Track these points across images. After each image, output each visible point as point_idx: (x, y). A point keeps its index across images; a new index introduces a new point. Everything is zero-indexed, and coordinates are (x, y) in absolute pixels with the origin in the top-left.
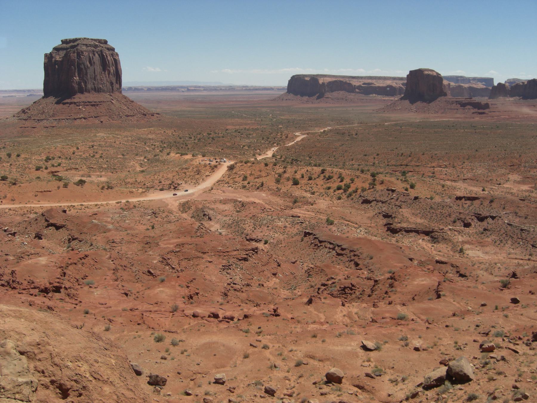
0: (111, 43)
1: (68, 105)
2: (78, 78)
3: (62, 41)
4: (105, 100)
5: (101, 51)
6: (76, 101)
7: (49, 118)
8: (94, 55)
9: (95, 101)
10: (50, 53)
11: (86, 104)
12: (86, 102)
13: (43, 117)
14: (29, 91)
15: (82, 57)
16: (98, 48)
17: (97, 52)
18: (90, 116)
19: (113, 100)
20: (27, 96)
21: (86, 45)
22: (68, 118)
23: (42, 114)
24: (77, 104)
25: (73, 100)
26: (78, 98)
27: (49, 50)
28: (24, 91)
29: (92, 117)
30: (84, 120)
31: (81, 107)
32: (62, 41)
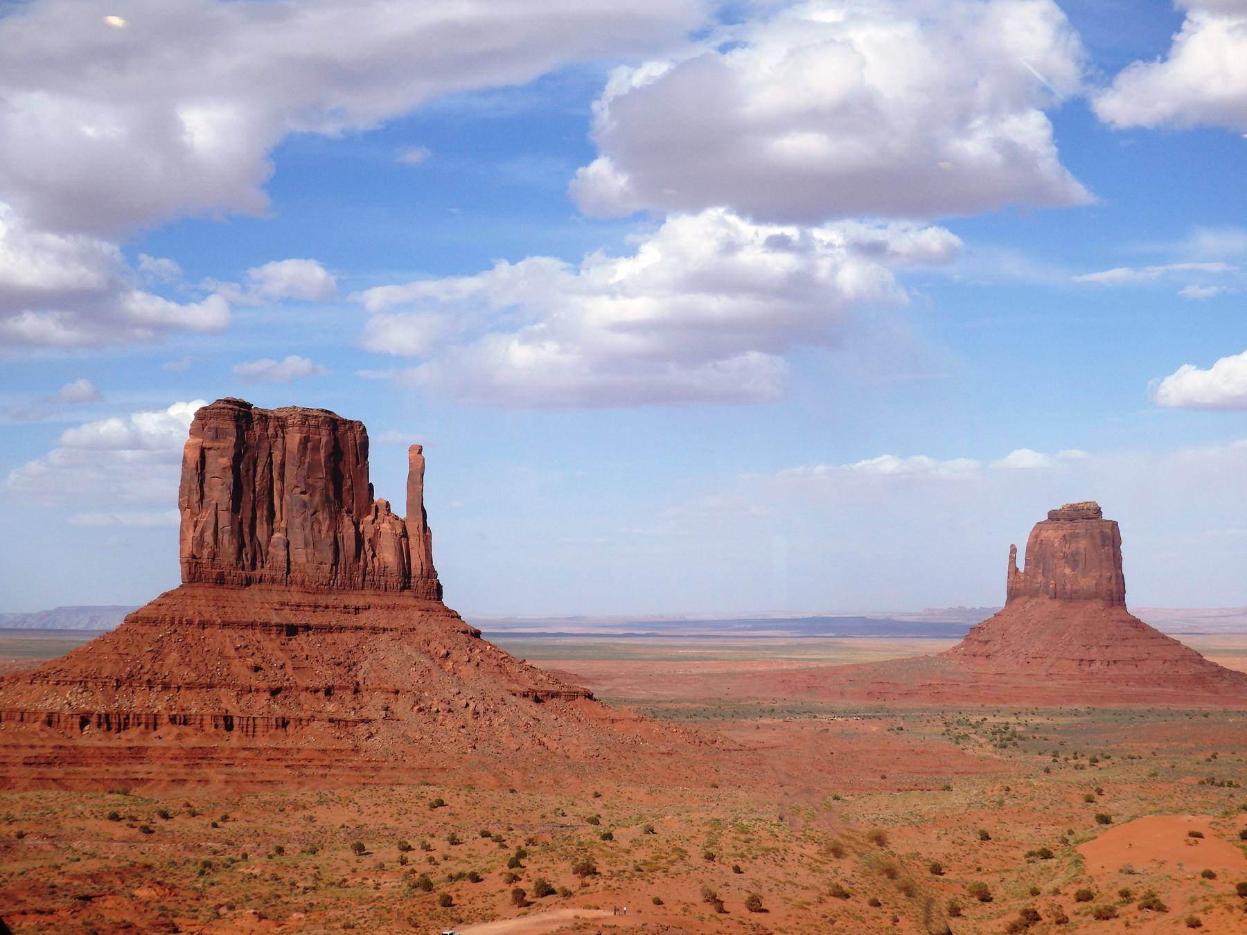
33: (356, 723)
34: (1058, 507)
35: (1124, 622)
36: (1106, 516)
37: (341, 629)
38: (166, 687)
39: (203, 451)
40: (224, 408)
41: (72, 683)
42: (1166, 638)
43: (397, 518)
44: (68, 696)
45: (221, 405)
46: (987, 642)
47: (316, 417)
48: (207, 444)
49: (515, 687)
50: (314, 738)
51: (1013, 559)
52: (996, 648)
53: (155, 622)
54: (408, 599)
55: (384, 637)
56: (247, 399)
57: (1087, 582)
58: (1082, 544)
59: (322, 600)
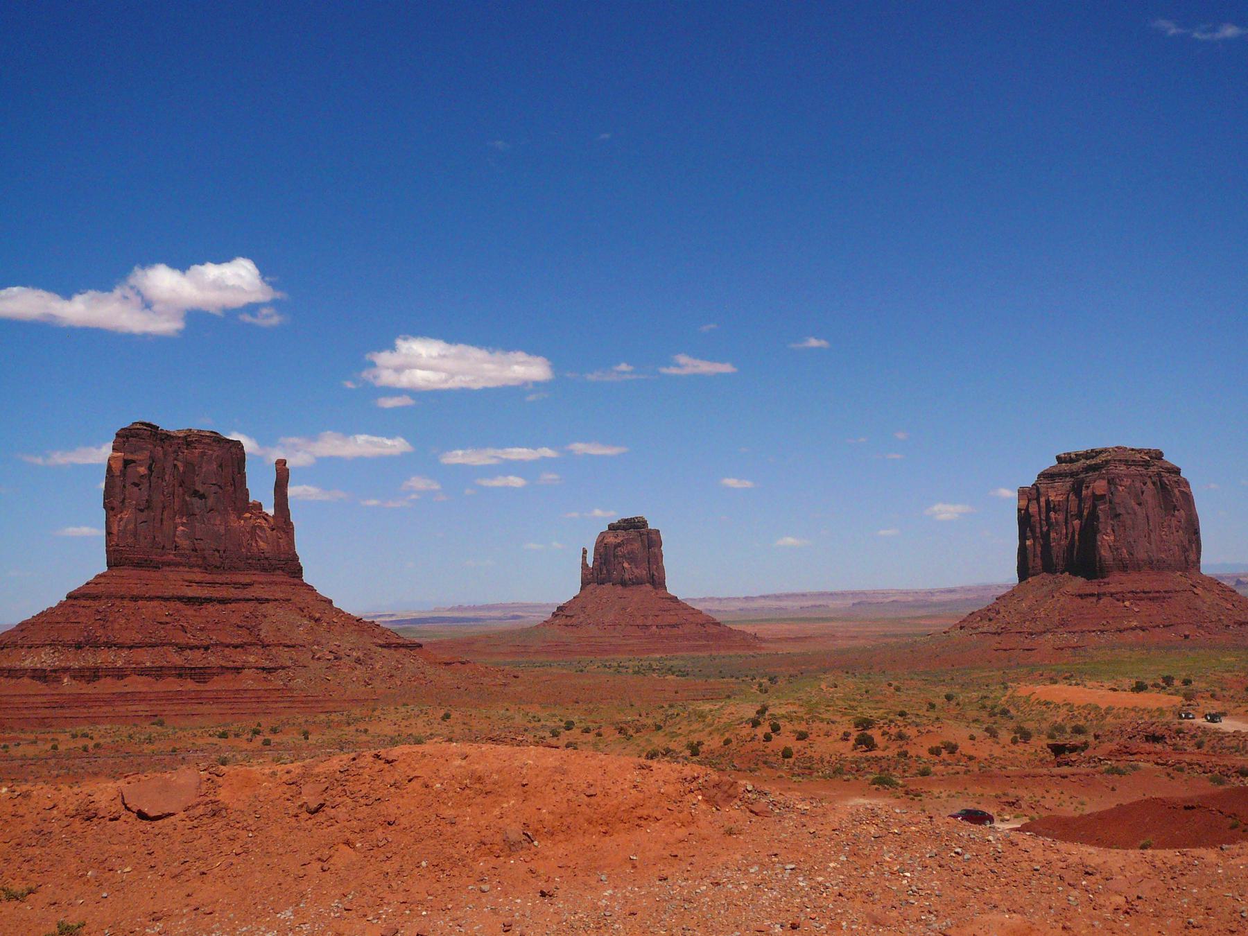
0: (1171, 458)
1: (1094, 599)
2: (1112, 538)
3: (1058, 458)
4: (1178, 589)
5: (1159, 474)
6: (1113, 591)
7: (1059, 630)
8: (1145, 484)
9: (1156, 589)
10: (1034, 485)
11: (1137, 596)
12: (1136, 593)
13: (1040, 626)
14: (854, 594)
15: (1120, 488)
16: (1152, 469)
17: (1150, 477)
18: (1154, 624)
19: (1195, 587)
20: (854, 604)
21: (1126, 462)
22: (1102, 627)
23: (1034, 620)
24: (1117, 596)
25: (1104, 589)
26: (1117, 582)
27: (1030, 481)
28: (843, 595)
29: (1158, 626)
30: (1141, 633)
31: (1127, 603)
32: (1058, 458)
33: (275, 669)
34: (615, 521)
35: (668, 598)
36: (650, 527)
37: (237, 600)
38: (121, 646)
39: (127, 463)
40: (138, 429)
41: (44, 645)
42: (694, 609)
43: (267, 515)
44: (43, 656)
45: (138, 426)
46: (572, 616)
47: (208, 436)
48: (130, 457)
49: (375, 640)
50: (249, 681)
51: (584, 558)
52: (580, 620)
53: (96, 597)
54: (280, 577)
55: (269, 606)
56: (154, 423)
57: (641, 572)
58: (637, 546)
59: (219, 579)
